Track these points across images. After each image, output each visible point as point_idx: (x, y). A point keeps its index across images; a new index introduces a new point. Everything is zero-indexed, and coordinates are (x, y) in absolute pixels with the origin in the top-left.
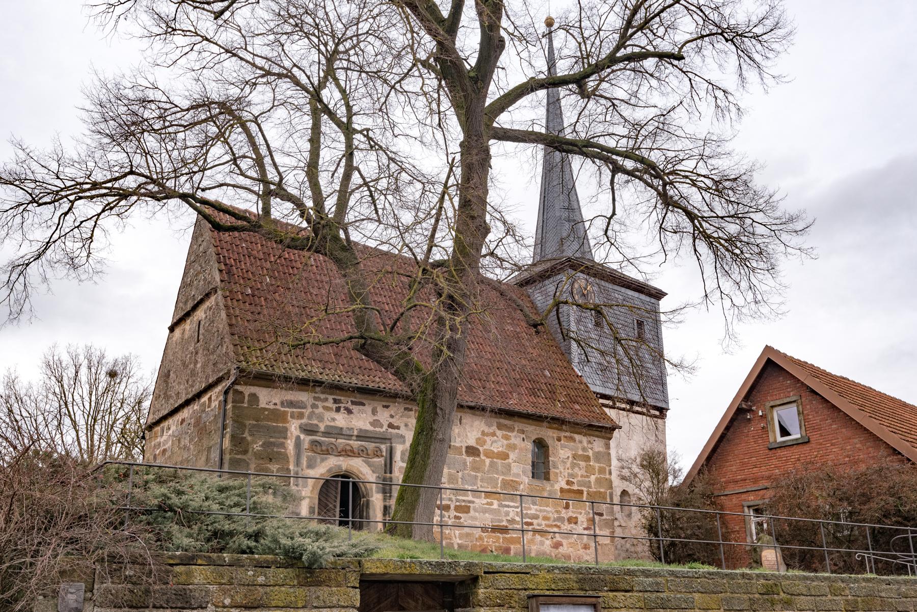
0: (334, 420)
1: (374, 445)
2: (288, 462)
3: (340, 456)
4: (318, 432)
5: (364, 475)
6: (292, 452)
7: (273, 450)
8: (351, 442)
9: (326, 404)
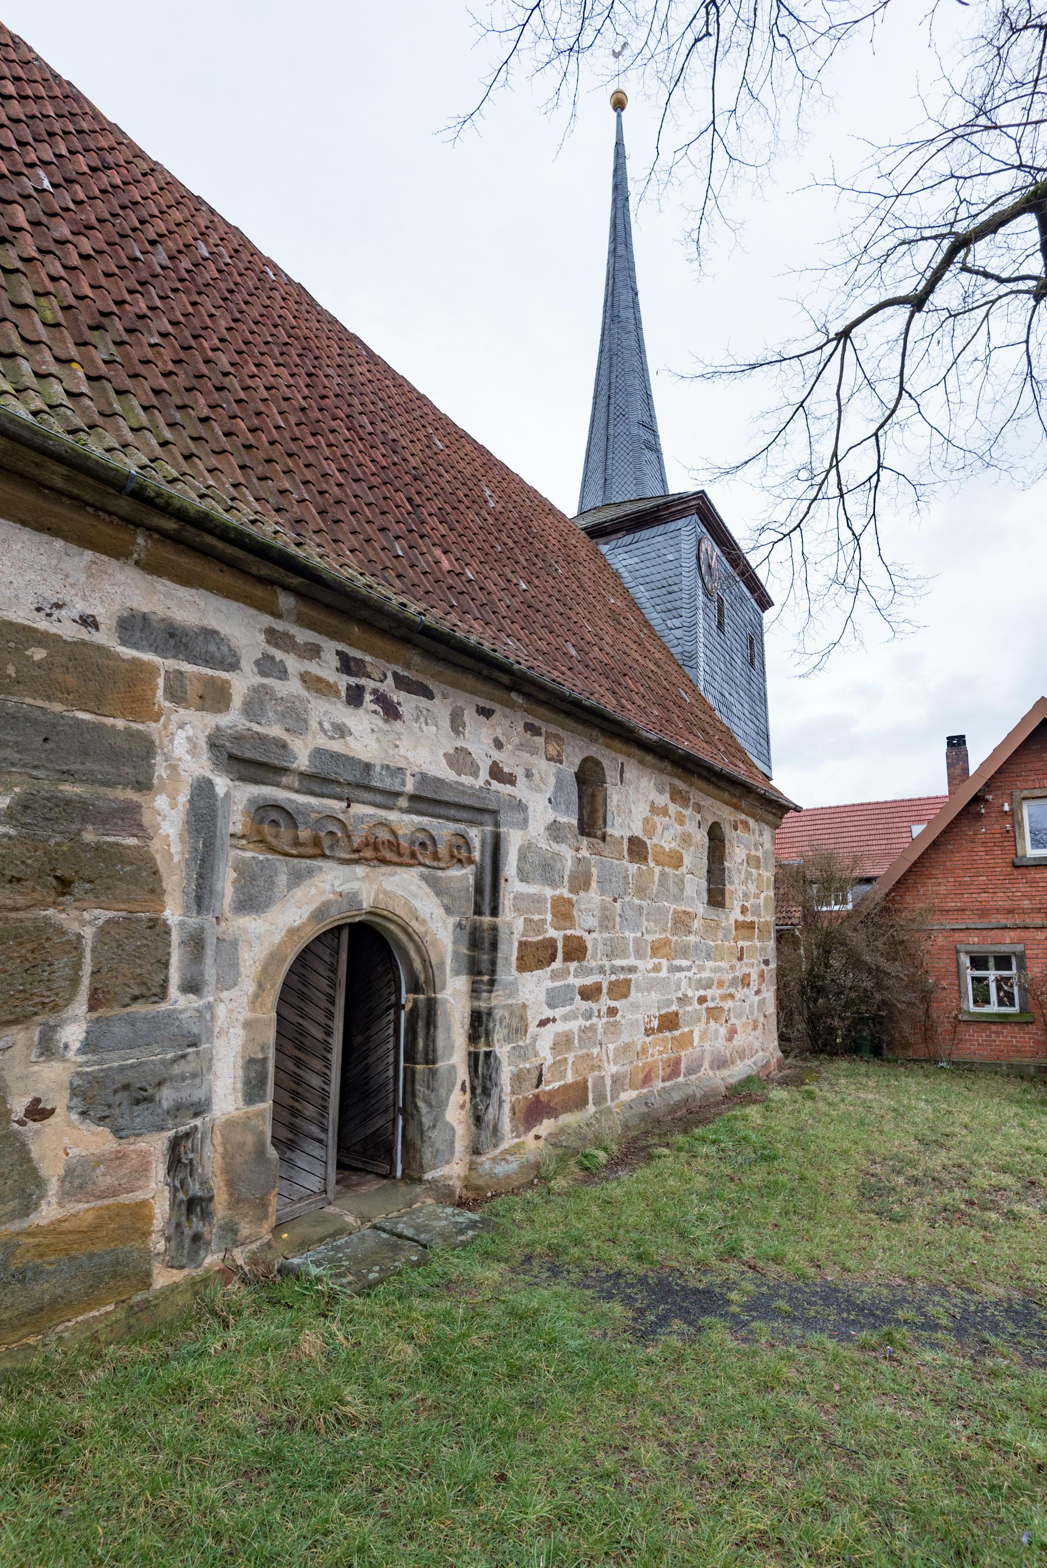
0: (341, 731)
1: (452, 827)
2: (156, 892)
3: (357, 862)
4: (285, 770)
5: (424, 922)
6: (176, 848)
7: (75, 838)
8: (393, 816)
9: (313, 668)
